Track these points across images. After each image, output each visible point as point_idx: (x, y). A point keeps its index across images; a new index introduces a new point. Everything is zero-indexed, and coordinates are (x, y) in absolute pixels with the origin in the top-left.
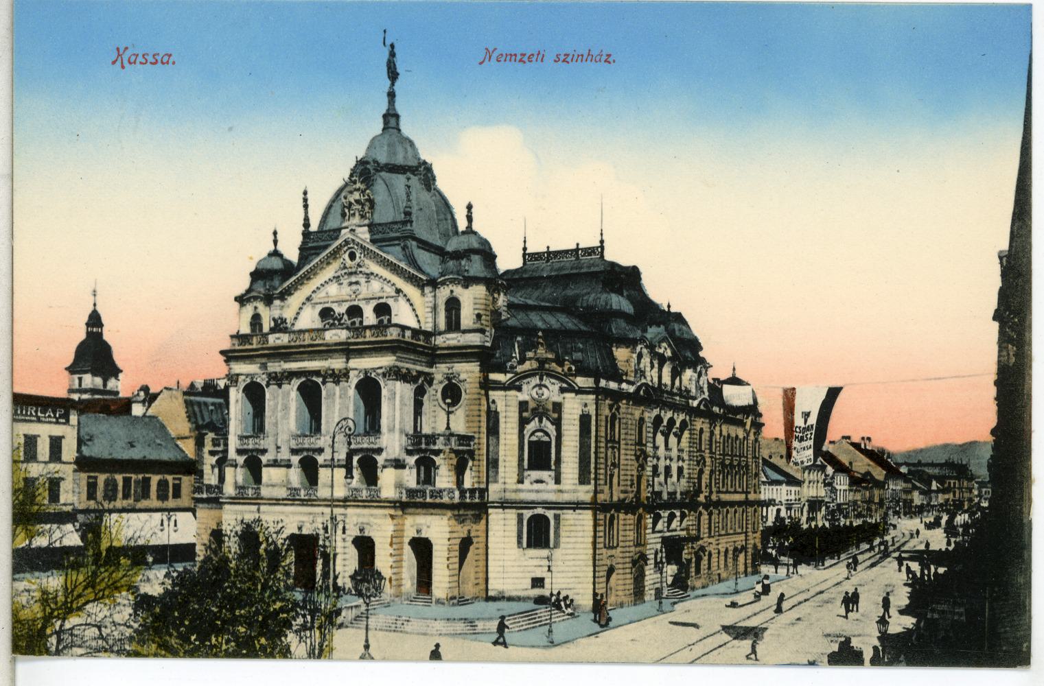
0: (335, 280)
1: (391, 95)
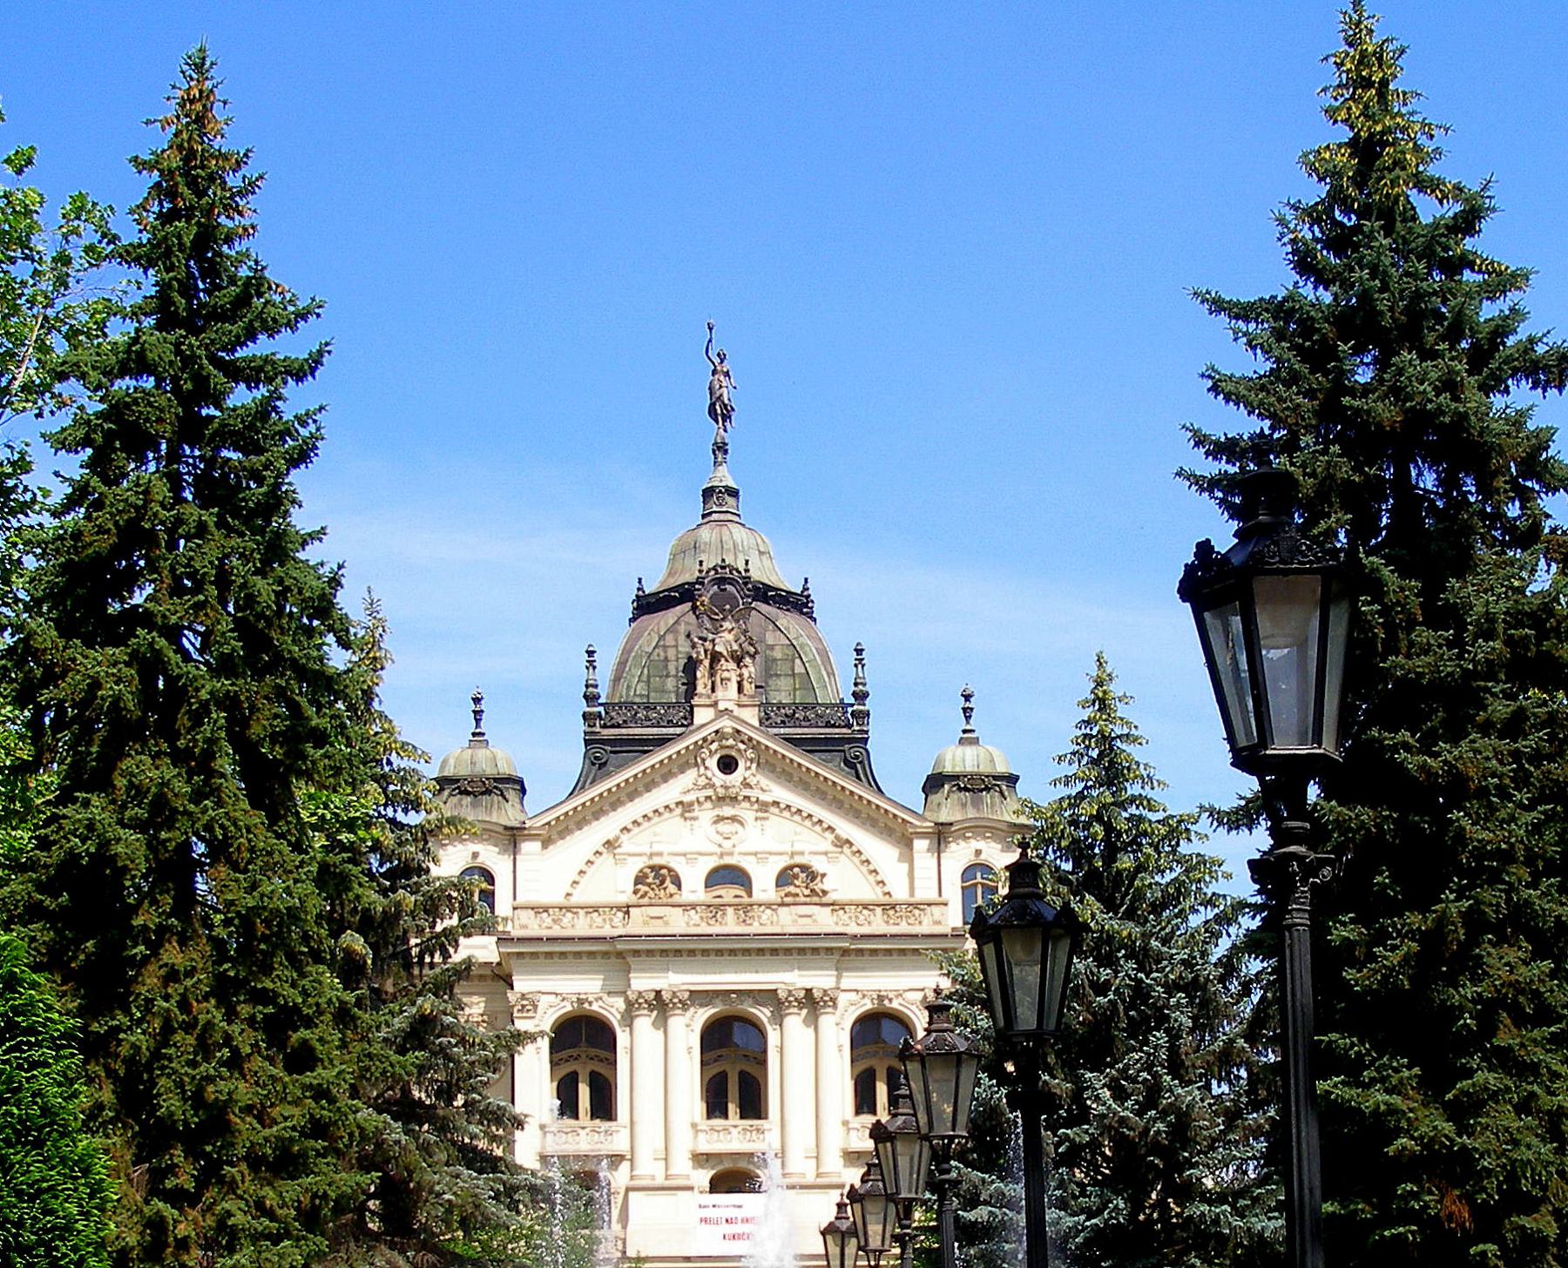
0: (679, 810)
1: (721, 448)
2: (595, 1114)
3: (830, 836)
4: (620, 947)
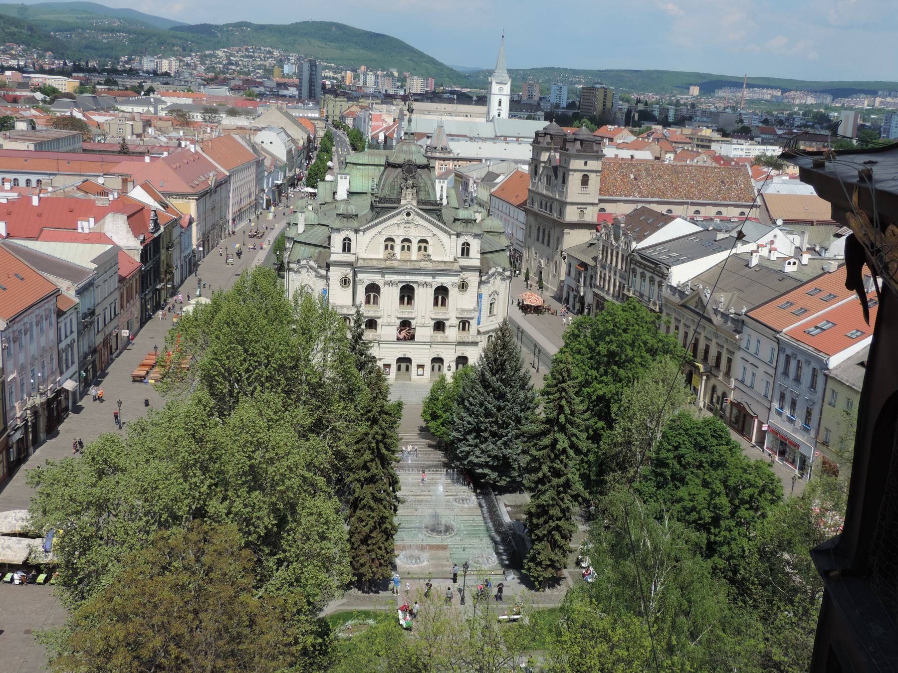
2: (374, 303)
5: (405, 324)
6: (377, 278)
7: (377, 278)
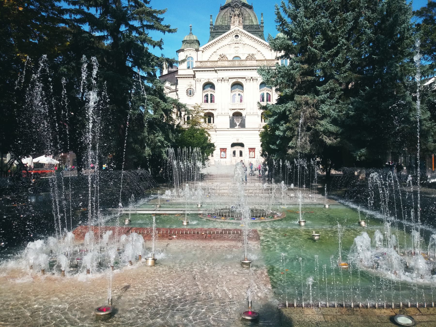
2: (212, 101)
3: (256, 50)
4: (216, 69)
5: (237, 115)
6: (211, 77)
7: (211, 77)
